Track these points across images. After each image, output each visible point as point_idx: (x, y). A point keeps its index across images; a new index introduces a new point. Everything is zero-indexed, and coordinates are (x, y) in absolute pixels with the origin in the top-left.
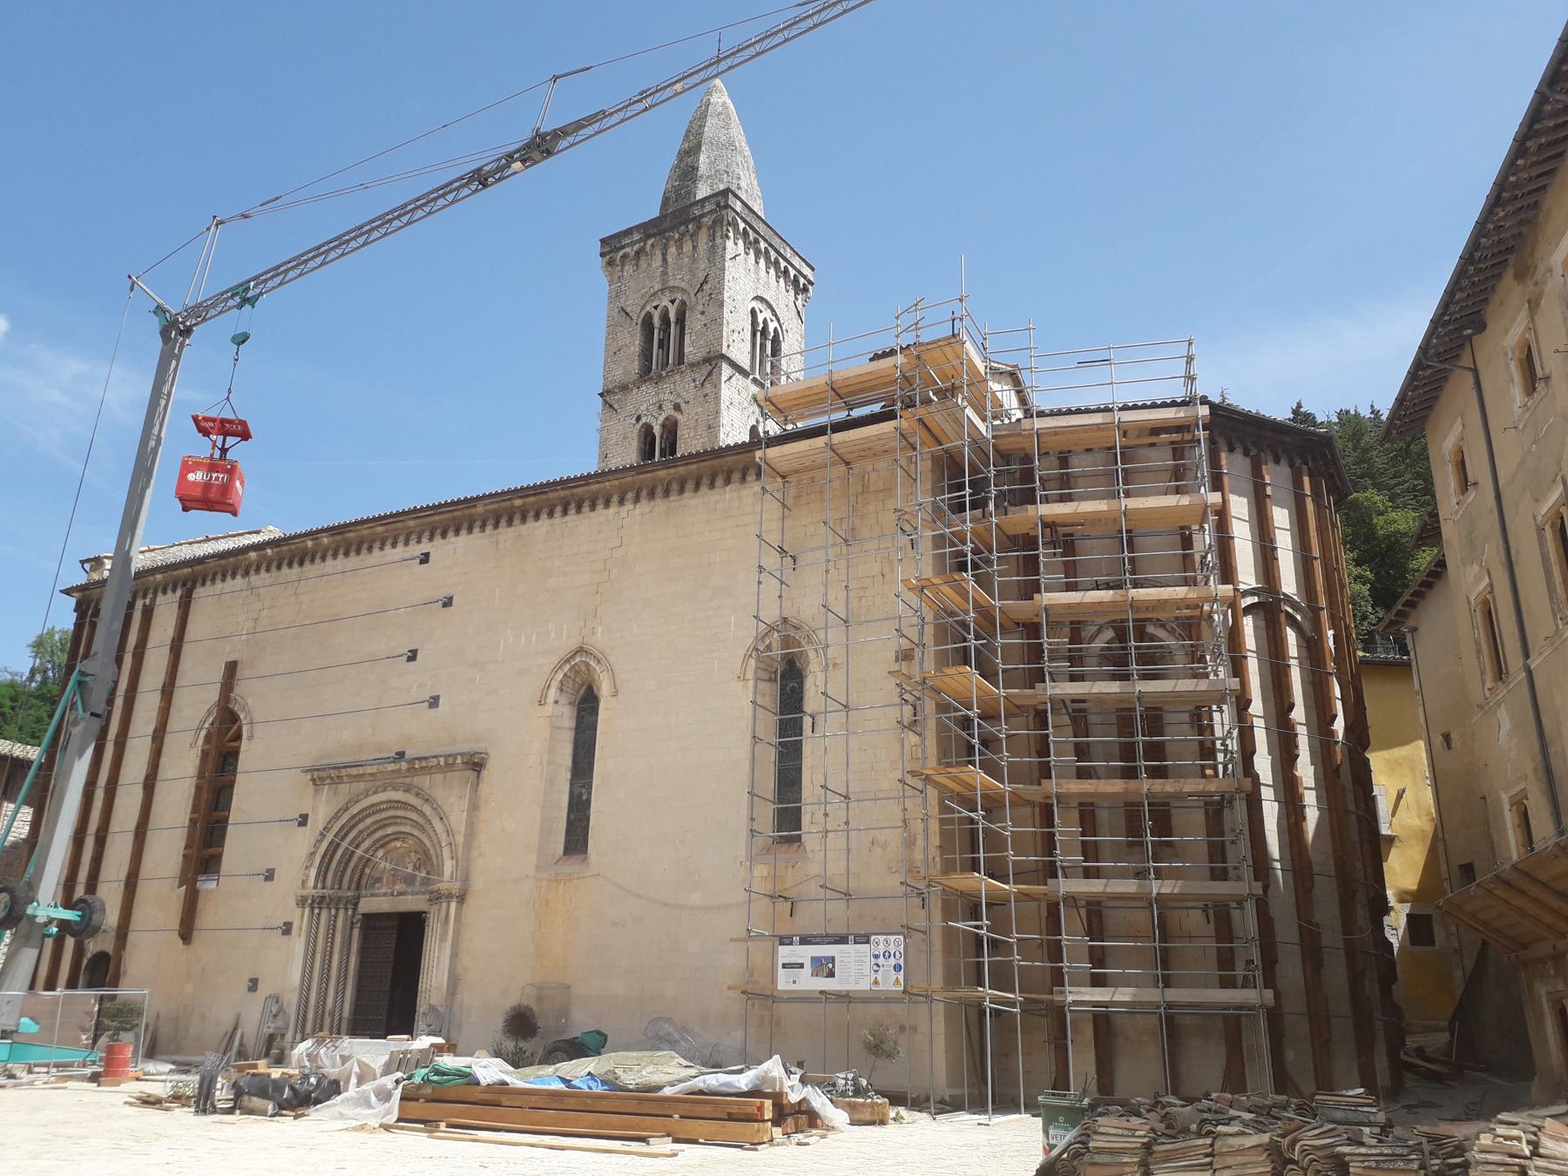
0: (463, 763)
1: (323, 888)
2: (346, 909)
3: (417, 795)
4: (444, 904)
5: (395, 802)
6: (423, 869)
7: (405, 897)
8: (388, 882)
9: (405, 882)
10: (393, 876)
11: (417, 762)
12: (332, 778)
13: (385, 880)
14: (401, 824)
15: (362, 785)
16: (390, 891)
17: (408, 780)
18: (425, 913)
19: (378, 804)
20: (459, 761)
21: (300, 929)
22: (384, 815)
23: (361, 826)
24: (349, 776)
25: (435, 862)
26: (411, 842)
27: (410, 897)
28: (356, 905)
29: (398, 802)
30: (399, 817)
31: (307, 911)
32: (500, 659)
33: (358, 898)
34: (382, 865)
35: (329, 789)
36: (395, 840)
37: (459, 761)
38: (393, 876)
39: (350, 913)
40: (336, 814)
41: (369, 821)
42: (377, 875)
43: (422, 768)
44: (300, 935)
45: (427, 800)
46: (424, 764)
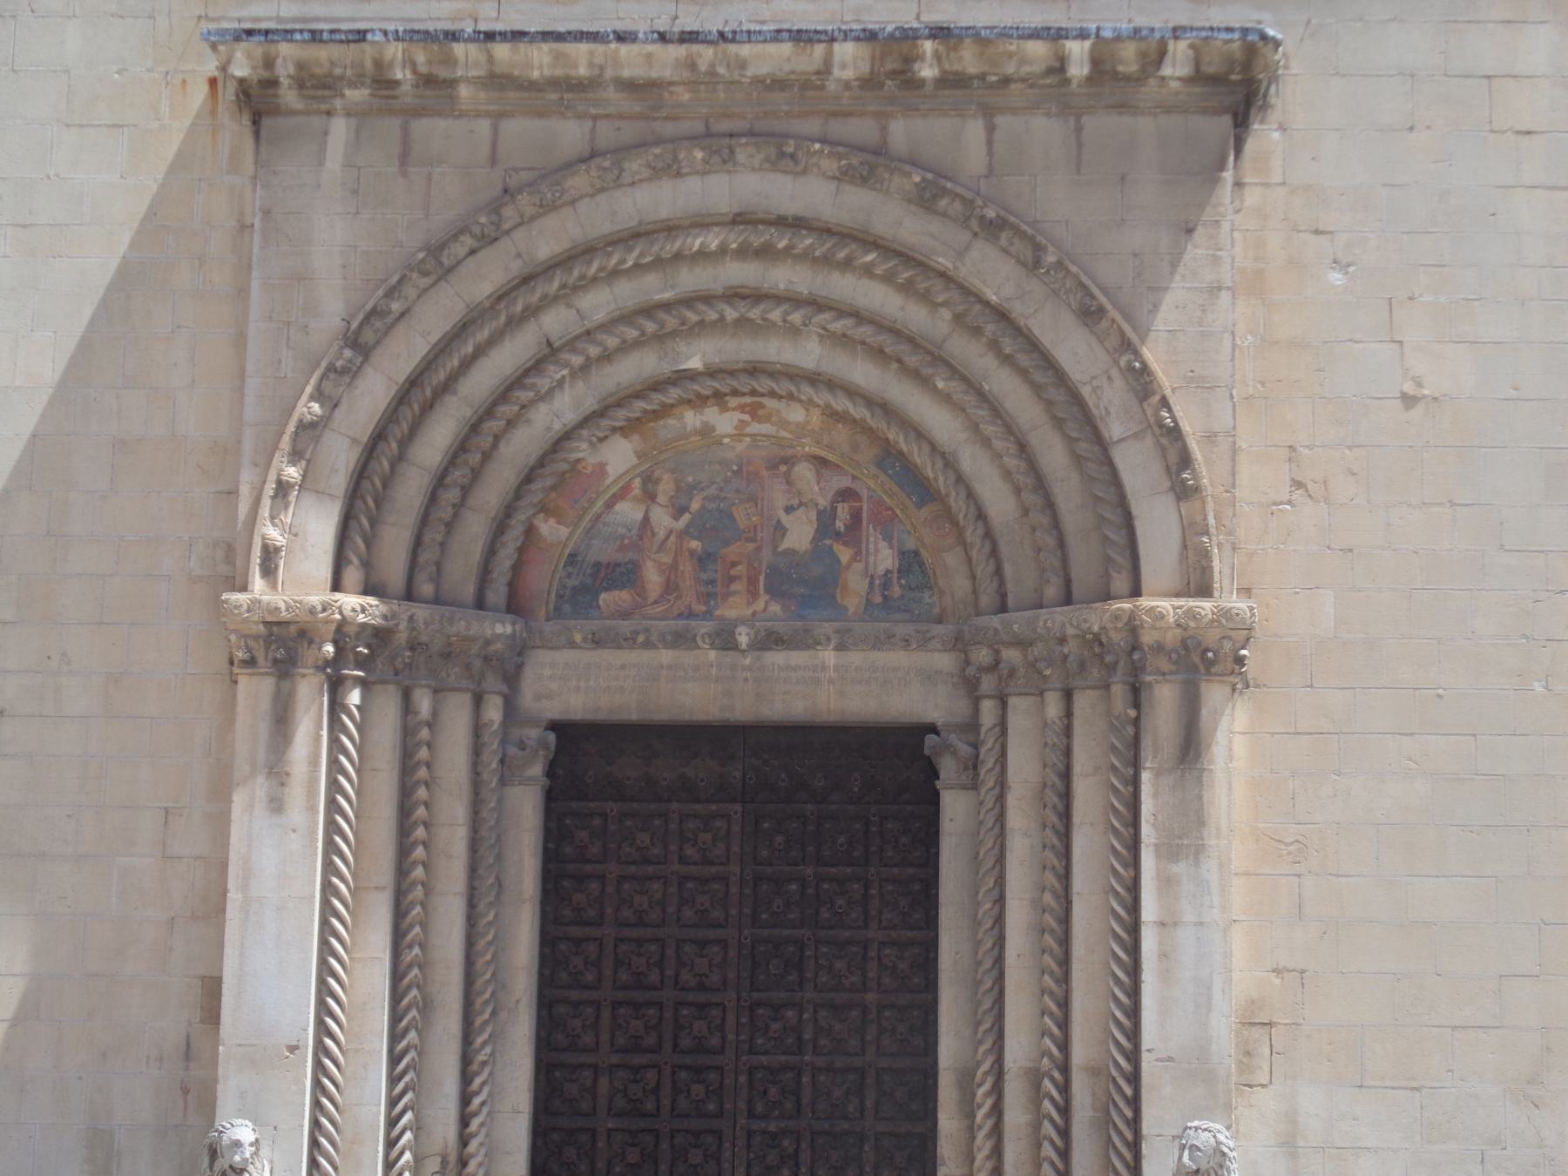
0: (1198, 77)
2: (478, 700)
3: (927, 199)
4: (1165, 697)
5: (781, 222)
6: (872, 537)
7: (798, 657)
8: (670, 587)
9: (774, 592)
10: (703, 560)
11: (928, 46)
12: (383, 83)
13: (653, 577)
14: (763, 328)
15: (570, 134)
17: (860, 129)
18: (932, 729)
19: (670, 228)
20: (1176, 66)
22: (690, 280)
23: (556, 322)
24: (496, 81)
25: (999, 501)
26: (796, 414)
27: (829, 656)
28: (512, 678)
29: (797, 224)
30: (778, 299)
33: (520, 650)
34: (629, 512)
35: (356, 143)
36: (698, 402)
37: (1176, 66)
38: (703, 560)
39: (494, 713)
40: (435, 250)
41: (598, 303)
42: (601, 551)
43: (952, 81)
45: (993, 228)
46: (968, 60)
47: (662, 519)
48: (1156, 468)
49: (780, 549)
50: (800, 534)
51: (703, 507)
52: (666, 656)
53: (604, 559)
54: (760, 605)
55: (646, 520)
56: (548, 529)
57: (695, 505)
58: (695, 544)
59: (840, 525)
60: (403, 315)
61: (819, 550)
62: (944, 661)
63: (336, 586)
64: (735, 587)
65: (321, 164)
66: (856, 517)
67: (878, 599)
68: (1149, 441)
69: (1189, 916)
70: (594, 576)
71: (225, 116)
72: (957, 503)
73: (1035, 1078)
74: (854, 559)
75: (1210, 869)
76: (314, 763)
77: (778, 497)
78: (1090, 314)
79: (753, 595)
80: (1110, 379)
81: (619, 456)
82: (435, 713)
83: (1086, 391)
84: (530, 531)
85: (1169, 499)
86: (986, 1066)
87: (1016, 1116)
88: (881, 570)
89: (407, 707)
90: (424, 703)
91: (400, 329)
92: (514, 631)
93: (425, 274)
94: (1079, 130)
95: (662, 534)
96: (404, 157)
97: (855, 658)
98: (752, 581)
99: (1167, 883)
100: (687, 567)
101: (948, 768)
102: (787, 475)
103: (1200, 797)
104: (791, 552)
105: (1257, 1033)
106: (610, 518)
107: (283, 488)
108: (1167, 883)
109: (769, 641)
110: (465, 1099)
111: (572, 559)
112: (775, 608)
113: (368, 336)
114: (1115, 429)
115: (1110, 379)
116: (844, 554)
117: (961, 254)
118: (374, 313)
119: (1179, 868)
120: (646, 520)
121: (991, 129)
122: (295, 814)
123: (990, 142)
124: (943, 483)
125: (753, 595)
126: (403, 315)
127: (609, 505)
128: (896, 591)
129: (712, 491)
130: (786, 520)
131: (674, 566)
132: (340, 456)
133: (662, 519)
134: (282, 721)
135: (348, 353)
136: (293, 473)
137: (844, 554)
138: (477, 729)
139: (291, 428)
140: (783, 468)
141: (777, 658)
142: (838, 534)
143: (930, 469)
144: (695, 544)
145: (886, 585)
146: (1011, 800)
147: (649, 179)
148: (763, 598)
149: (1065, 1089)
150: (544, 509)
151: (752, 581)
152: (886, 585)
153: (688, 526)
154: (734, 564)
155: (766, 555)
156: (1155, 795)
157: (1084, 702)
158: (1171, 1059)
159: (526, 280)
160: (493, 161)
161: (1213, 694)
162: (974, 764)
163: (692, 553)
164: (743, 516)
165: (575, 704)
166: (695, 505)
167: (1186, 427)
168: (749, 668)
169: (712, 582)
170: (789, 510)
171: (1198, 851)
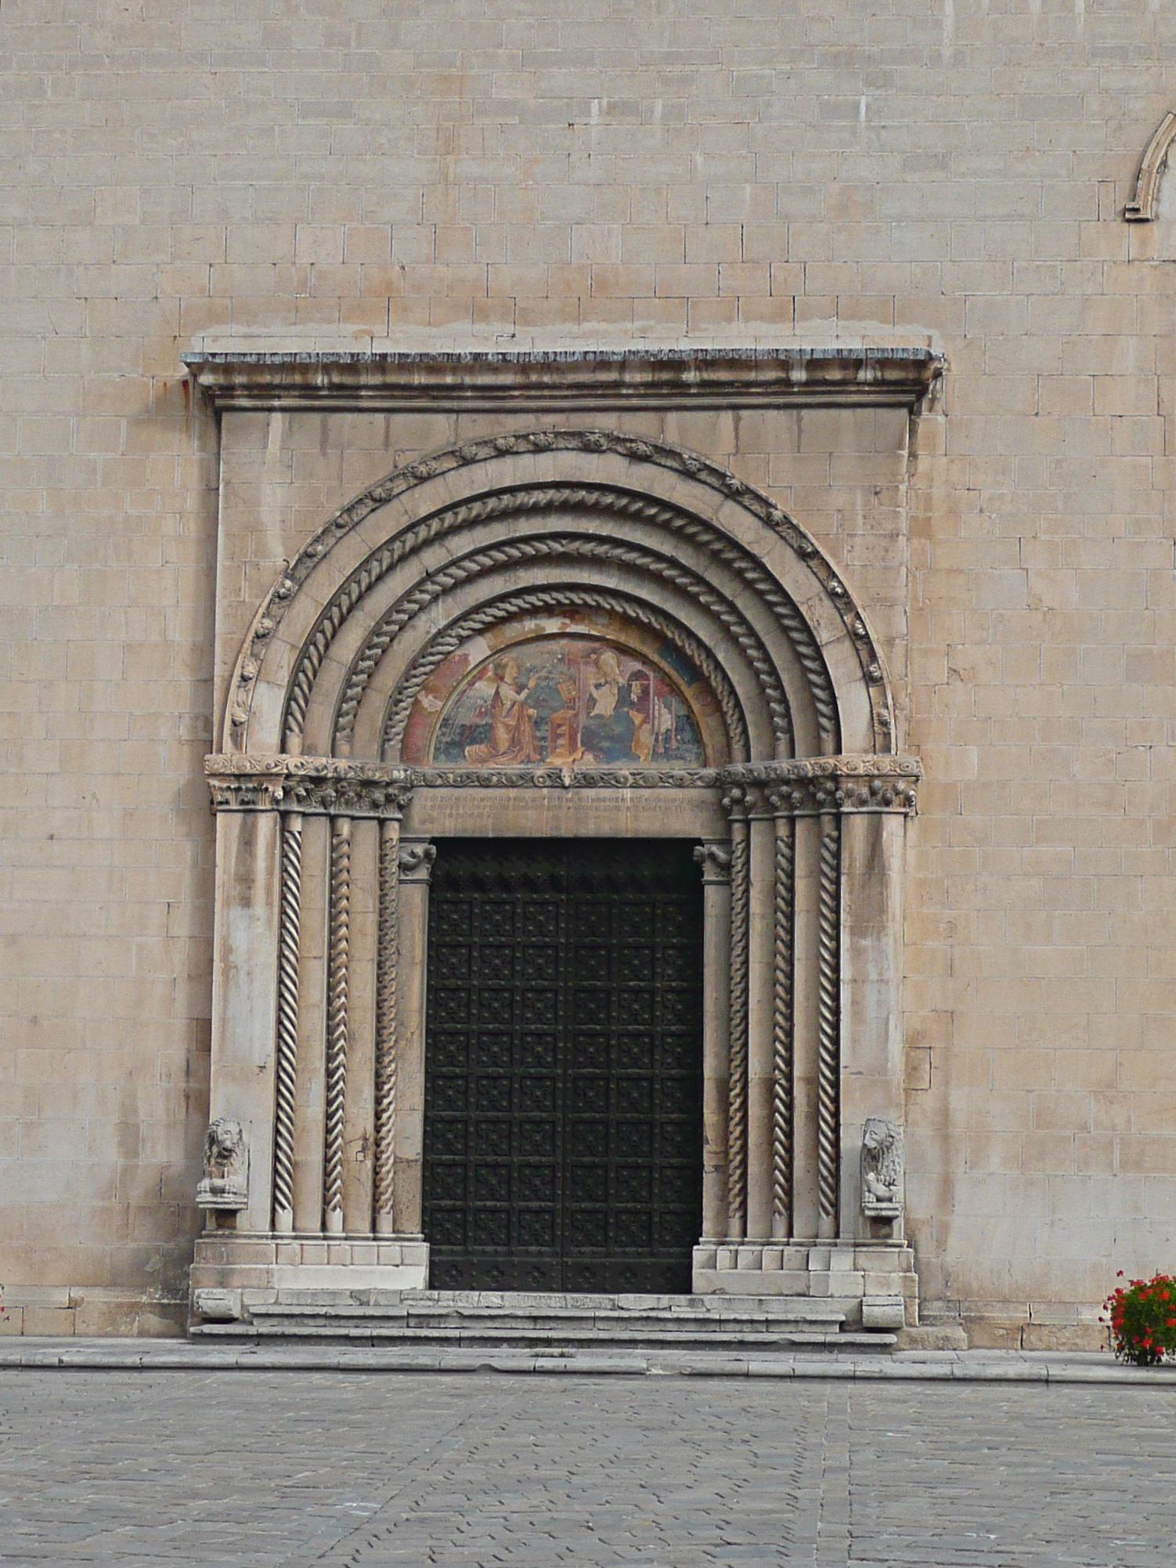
1: (306, 750)
4: (857, 827)
6: (657, 706)
8: (514, 742)
9: (589, 745)
10: (537, 724)
13: (502, 735)
16: (540, 771)
21: (246, 879)
27: (628, 793)
31: (266, 825)
32: (947, 53)
34: (485, 689)
35: (289, 432)
38: (537, 724)
40: (349, 510)
42: (466, 717)
44: (246, 902)
47: (508, 692)
48: (853, 663)
49: (592, 715)
50: (606, 703)
51: (537, 685)
52: (512, 793)
53: (467, 723)
54: (578, 755)
55: (497, 693)
56: (427, 701)
57: (532, 684)
58: (531, 711)
59: (634, 697)
60: (325, 556)
61: (618, 715)
62: (709, 794)
63: (283, 749)
64: (560, 742)
65: (265, 447)
66: (645, 691)
67: (661, 750)
68: (847, 644)
69: (874, 976)
70: (461, 734)
71: (195, 410)
72: (715, 681)
73: (769, 1084)
74: (644, 721)
75: (888, 942)
76: (270, 873)
77: (590, 676)
78: (807, 555)
79: (573, 748)
80: (821, 599)
81: (478, 650)
82: (352, 834)
83: (803, 609)
84: (417, 703)
85: (862, 685)
86: (736, 1077)
87: (755, 1111)
88: (663, 729)
89: (334, 833)
90: (345, 827)
91: (324, 566)
92: (406, 777)
93: (339, 526)
94: (800, 420)
95: (509, 704)
96: (324, 442)
97: (646, 793)
98: (572, 738)
99: (857, 952)
100: (526, 728)
101: (710, 874)
102: (596, 663)
103: (881, 894)
104: (599, 716)
105: (920, 1054)
106: (471, 693)
107: (244, 679)
108: (857, 952)
109: (587, 781)
110: (378, 1101)
111: (445, 723)
112: (589, 757)
113: (301, 573)
114: (823, 636)
115: (821, 599)
116: (637, 718)
117: (716, 512)
118: (308, 555)
119: (866, 942)
120: (497, 693)
121: (737, 421)
122: (259, 909)
123: (736, 429)
124: (706, 667)
125: (573, 748)
126: (325, 556)
127: (471, 684)
128: (674, 745)
129: (544, 673)
130: (595, 694)
131: (517, 728)
132: (282, 657)
133: (508, 692)
134: (247, 842)
135: (288, 583)
136: (251, 670)
137: (637, 718)
138: (382, 842)
139: (250, 637)
140: (594, 656)
141: (590, 793)
142: (632, 704)
143: (699, 659)
144: (531, 711)
145: (667, 740)
146: (753, 893)
147: (496, 457)
148: (581, 749)
149: (789, 1091)
150: (424, 686)
151: (572, 738)
152: (667, 740)
153: (527, 698)
154: (559, 726)
155: (583, 720)
156: (851, 892)
157: (799, 827)
158: (860, 1073)
159: (411, 528)
160: (387, 444)
161: (892, 825)
162: (726, 867)
163: (530, 717)
164: (566, 691)
165: (449, 827)
166: (532, 684)
167: (873, 636)
168: (571, 800)
169: (544, 738)
170: (598, 686)
171: (881, 929)
